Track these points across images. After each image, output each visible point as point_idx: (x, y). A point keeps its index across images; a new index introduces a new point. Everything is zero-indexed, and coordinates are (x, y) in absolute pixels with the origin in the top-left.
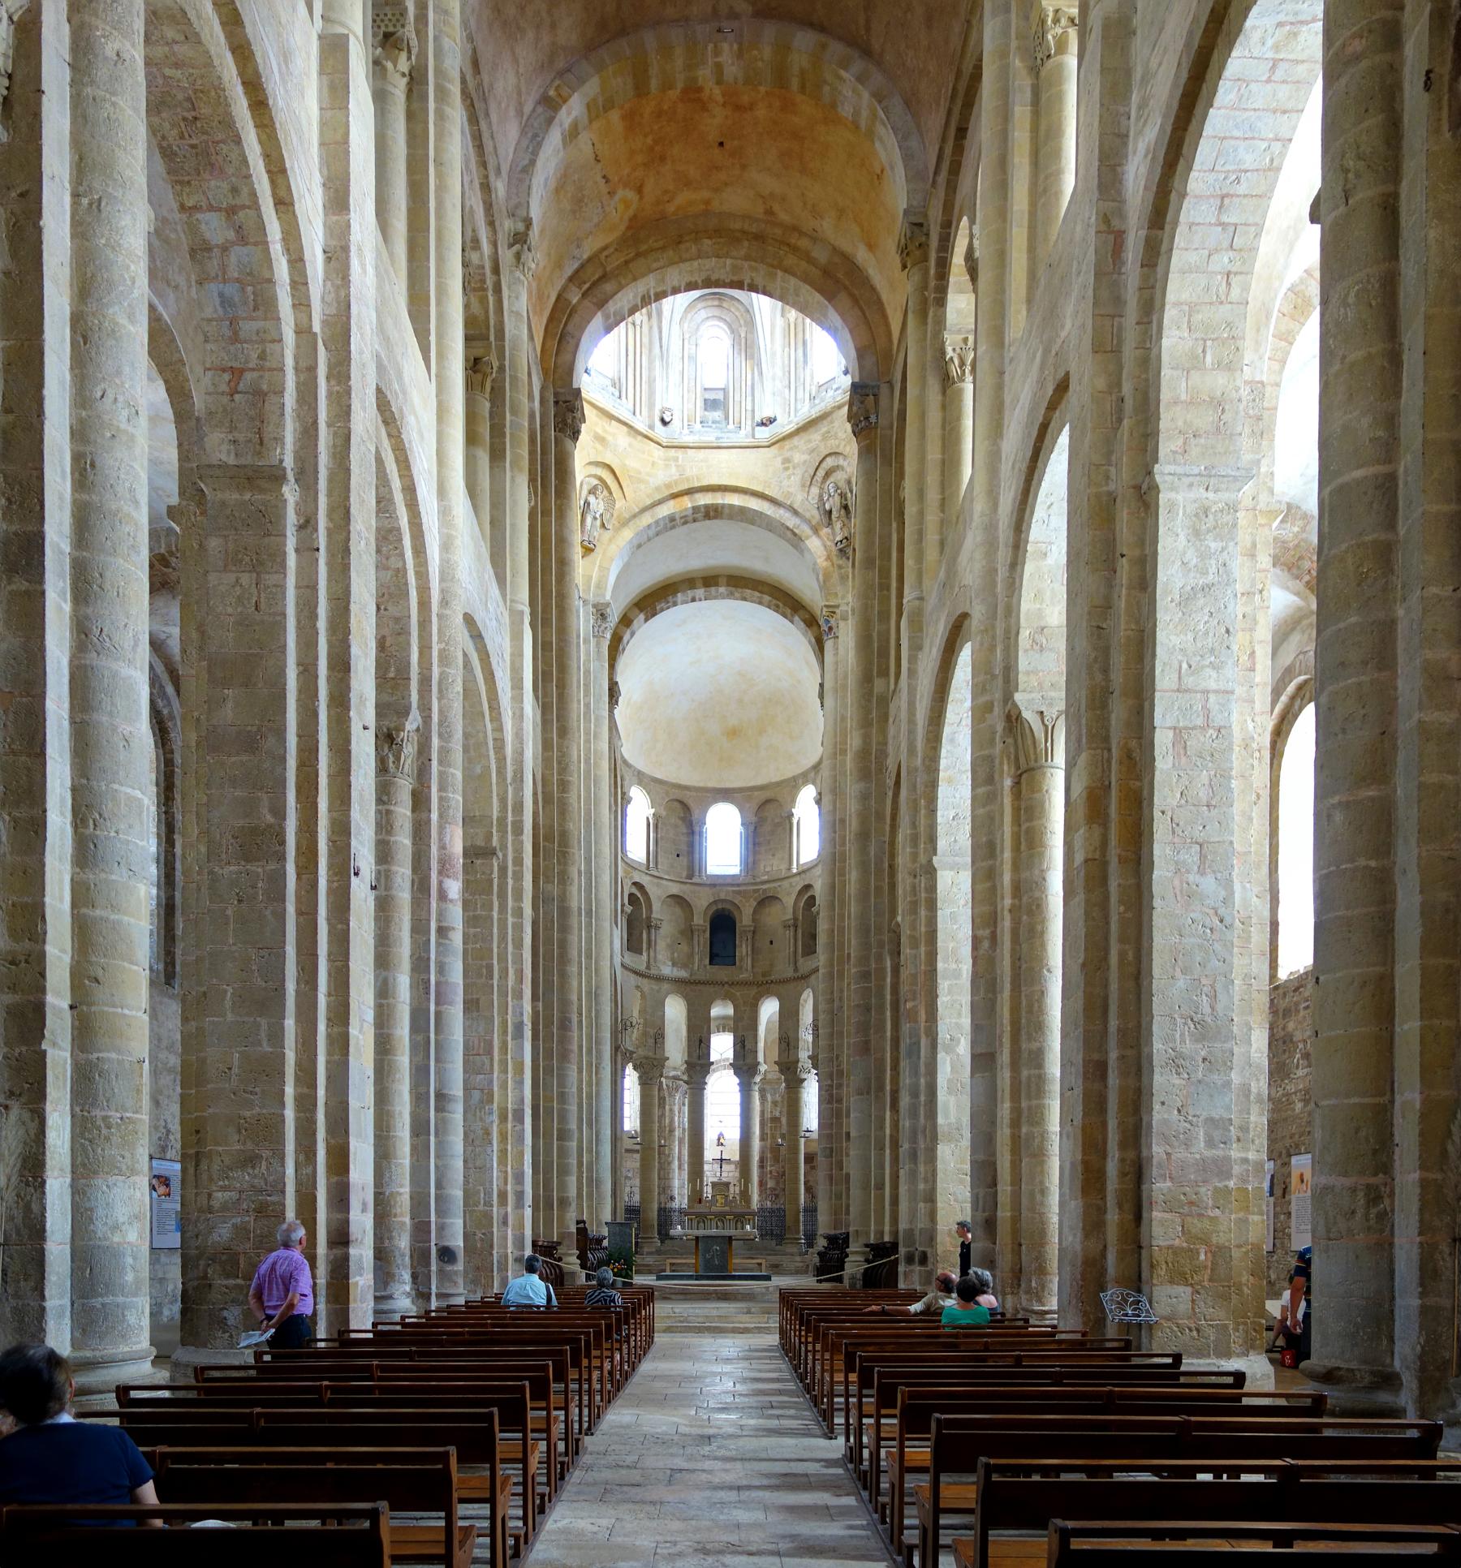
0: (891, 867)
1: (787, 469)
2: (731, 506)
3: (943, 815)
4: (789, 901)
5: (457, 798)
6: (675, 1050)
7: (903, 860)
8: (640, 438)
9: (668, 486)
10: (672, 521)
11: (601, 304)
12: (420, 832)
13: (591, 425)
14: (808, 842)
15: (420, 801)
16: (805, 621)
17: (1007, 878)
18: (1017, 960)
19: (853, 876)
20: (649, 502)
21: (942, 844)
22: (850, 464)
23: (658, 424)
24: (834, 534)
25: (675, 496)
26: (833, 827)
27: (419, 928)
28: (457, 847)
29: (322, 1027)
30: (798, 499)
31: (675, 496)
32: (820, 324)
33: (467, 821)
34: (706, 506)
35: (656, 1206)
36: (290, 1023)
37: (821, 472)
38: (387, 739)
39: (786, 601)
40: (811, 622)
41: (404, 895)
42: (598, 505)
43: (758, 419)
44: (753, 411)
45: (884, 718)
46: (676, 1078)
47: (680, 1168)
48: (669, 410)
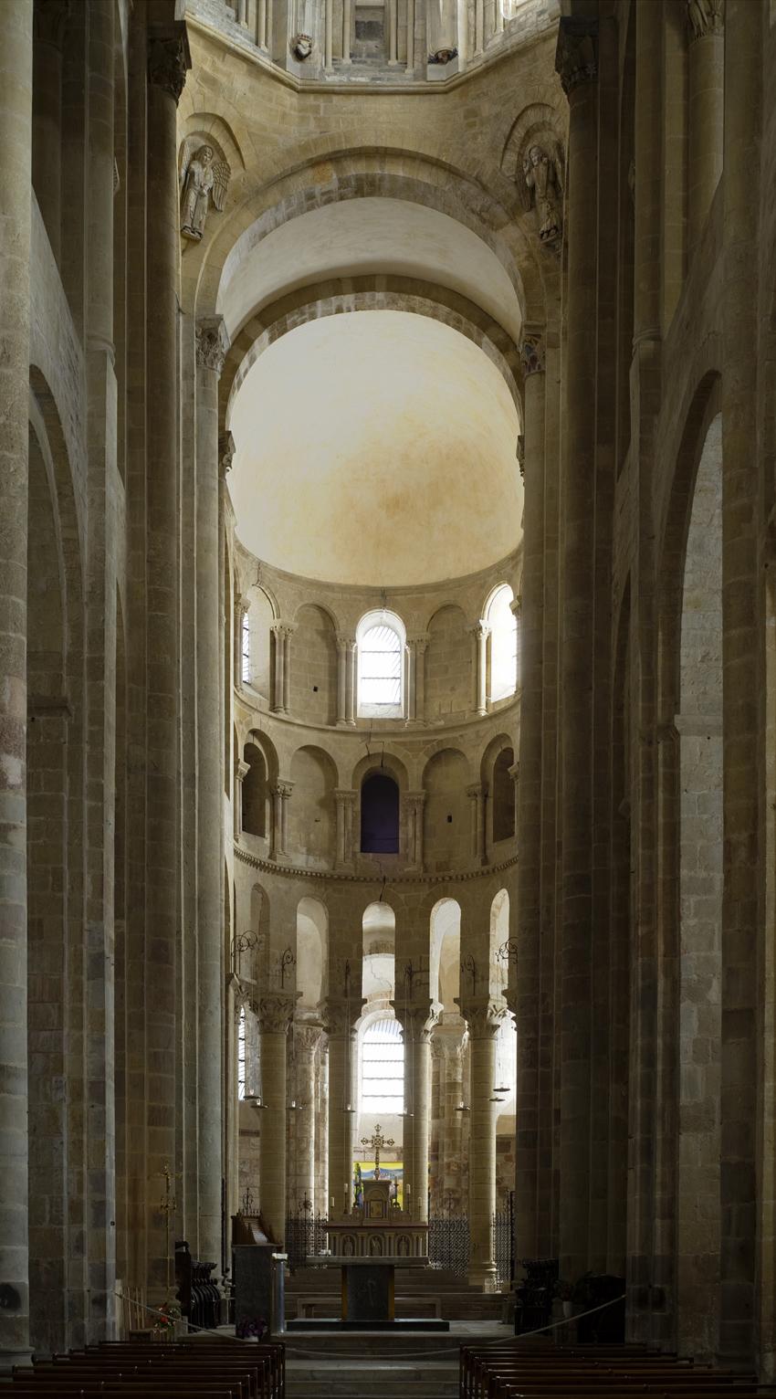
0: (619, 722)
1: (471, 125)
2: (394, 178)
4: (475, 755)
6: (310, 981)
8: (264, 79)
9: (304, 148)
14: (502, 673)
16: (497, 344)
19: (564, 735)
20: (277, 171)
23: (289, 56)
24: (539, 223)
25: (315, 163)
31: (315, 163)
34: (358, 179)
35: (283, 1217)
40: (504, 345)
42: (205, 176)
43: (430, 51)
44: (424, 40)
45: (608, 501)
46: (312, 1023)
47: (317, 1159)
48: (306, 38)
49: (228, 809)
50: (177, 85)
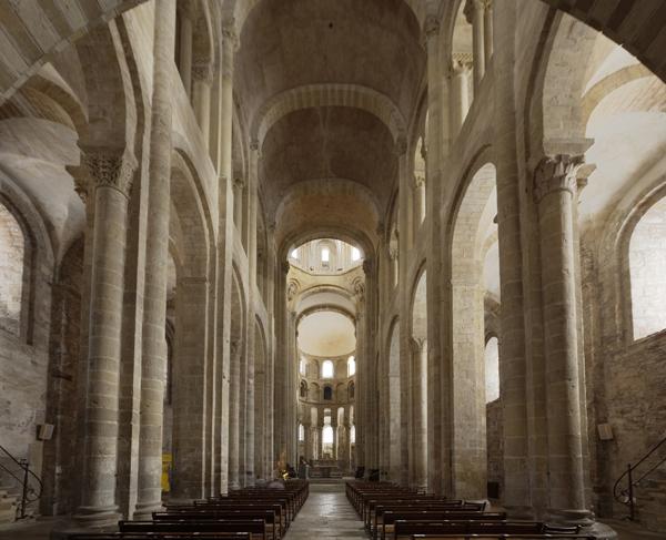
3: (391, 364)
5: (253, 359)
7: (380, 374)
10: (314, 293)
11: (295, 242)
12: (242, 367)
13: (291, 270)
15: (242, 360)
17: (410, 379)
18: (413, 400)
21: (391, 370)
22: (363, 276)
26: (359, 367)
27: (242, 391)
28: (253, 370)
29: (214, 417)
30: (349, 288)
32: (354, 245)
33: (256, 364)
36: (204, 416)
37: (356, 281)
38: (233, 344)
39: (345, 312)
41: (238, 383)
42: (293, 289)
49: (298, 393)
50: (287, 272)
